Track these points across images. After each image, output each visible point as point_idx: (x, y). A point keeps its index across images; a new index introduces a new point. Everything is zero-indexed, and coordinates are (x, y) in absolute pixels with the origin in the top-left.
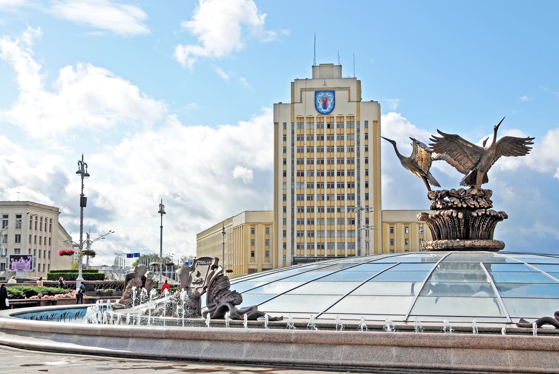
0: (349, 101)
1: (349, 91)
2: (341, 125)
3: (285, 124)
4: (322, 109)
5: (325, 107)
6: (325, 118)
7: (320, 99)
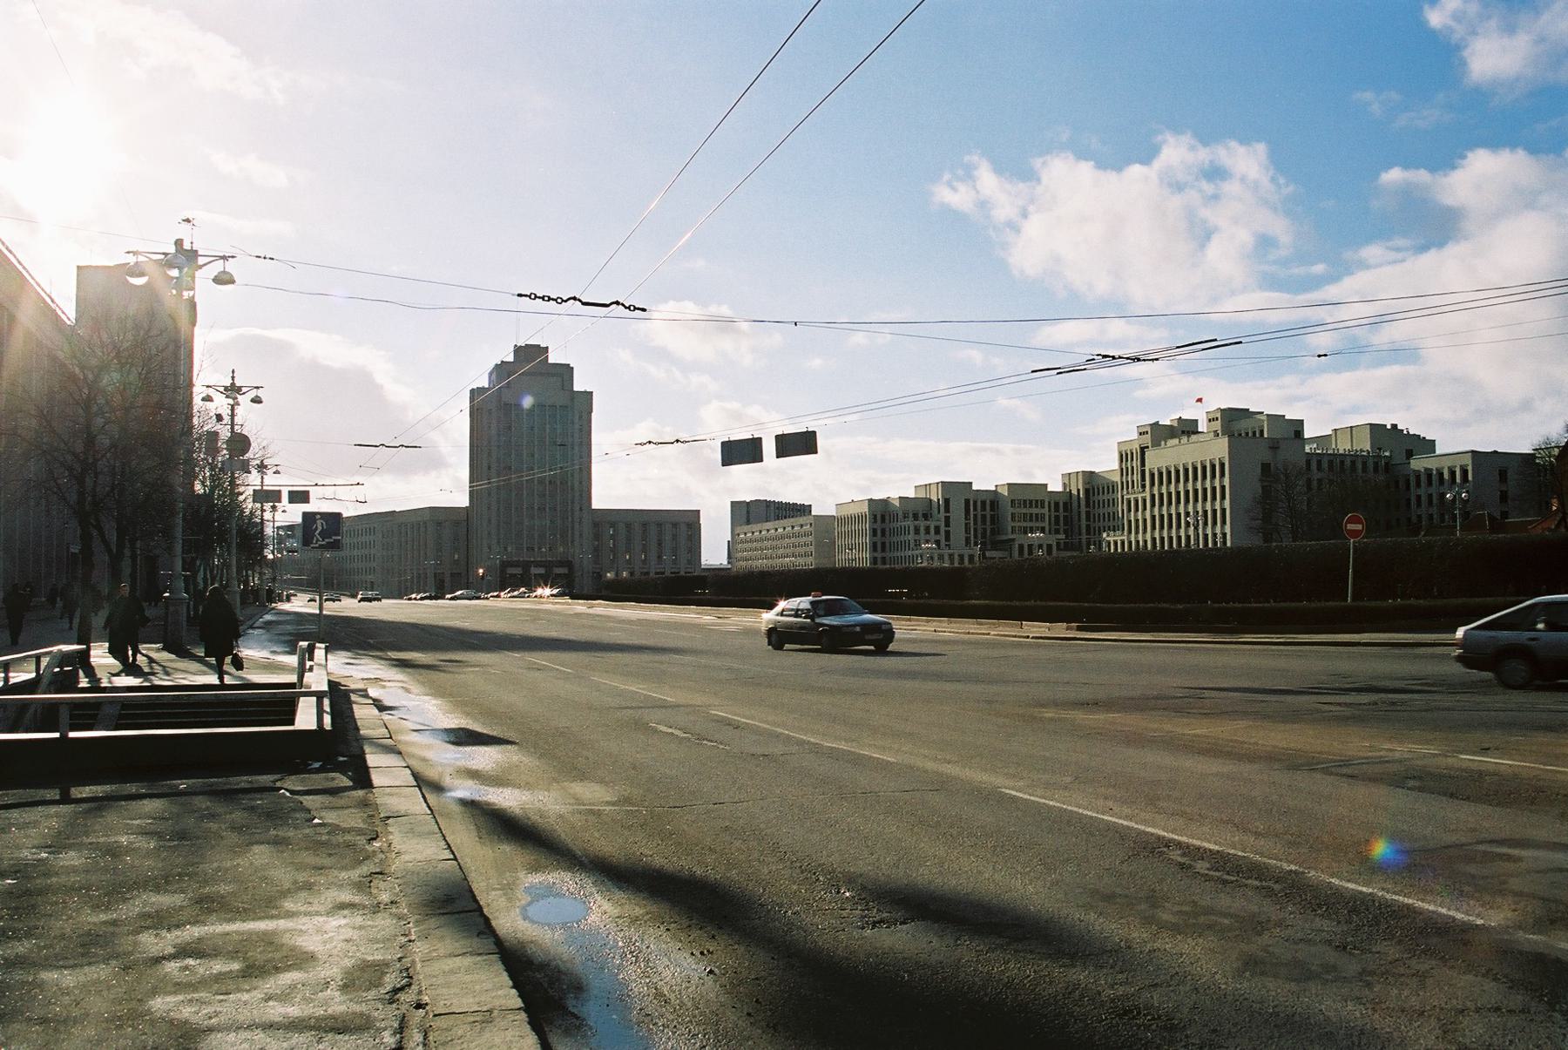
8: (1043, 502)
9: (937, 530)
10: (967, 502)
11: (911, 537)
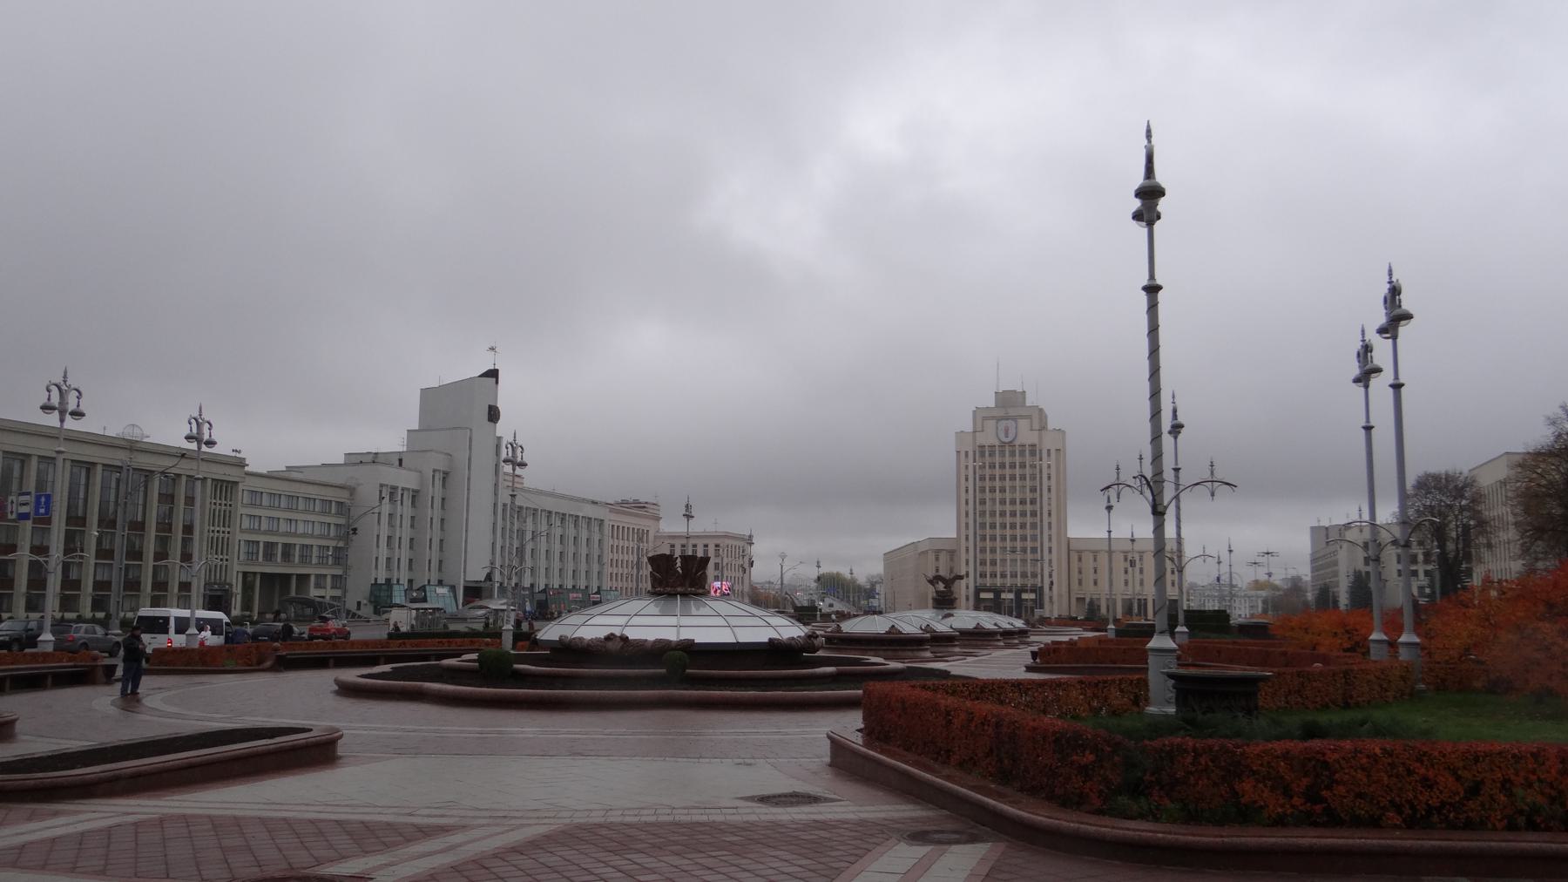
2: (1022, 453)
3: (967, 453)
5: (1007, 437)
6: (1007, 447)
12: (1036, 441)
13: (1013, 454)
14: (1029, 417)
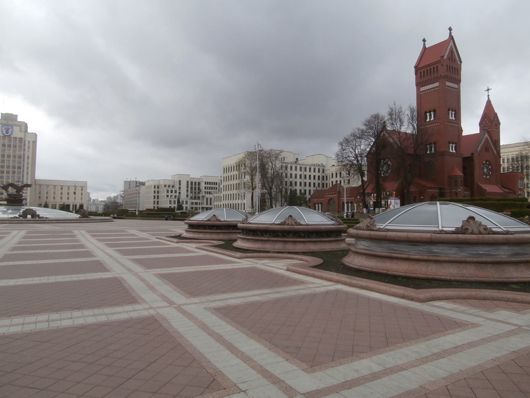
0: (21, 131)
1: (21, 127)
4: (5, 134)
5: (7, 132)
7: (4, 129)
8: (217, 183)
9: (176, 192)
10: (188, 182)
11: (166, 194)
12: (23, 137)
13: (10, 141)
14: (20, 126)
